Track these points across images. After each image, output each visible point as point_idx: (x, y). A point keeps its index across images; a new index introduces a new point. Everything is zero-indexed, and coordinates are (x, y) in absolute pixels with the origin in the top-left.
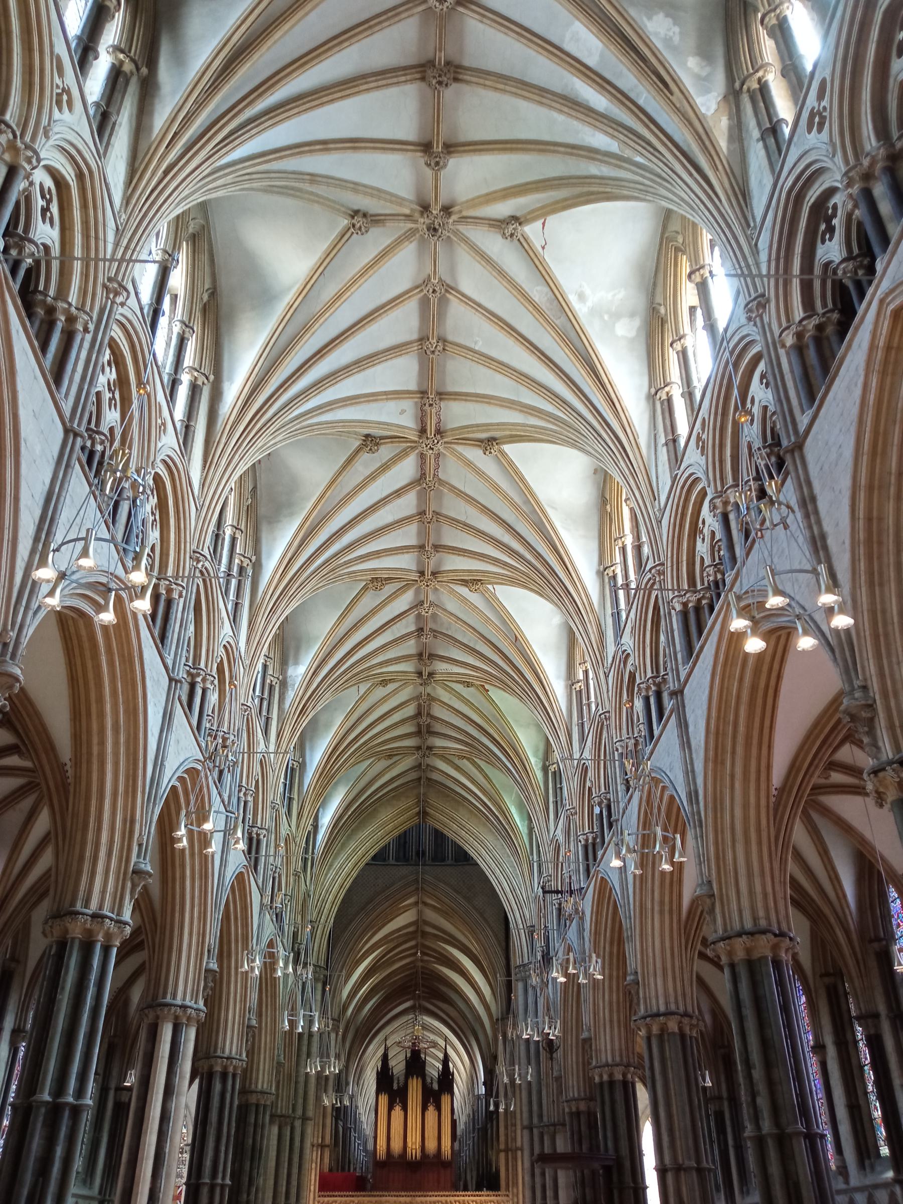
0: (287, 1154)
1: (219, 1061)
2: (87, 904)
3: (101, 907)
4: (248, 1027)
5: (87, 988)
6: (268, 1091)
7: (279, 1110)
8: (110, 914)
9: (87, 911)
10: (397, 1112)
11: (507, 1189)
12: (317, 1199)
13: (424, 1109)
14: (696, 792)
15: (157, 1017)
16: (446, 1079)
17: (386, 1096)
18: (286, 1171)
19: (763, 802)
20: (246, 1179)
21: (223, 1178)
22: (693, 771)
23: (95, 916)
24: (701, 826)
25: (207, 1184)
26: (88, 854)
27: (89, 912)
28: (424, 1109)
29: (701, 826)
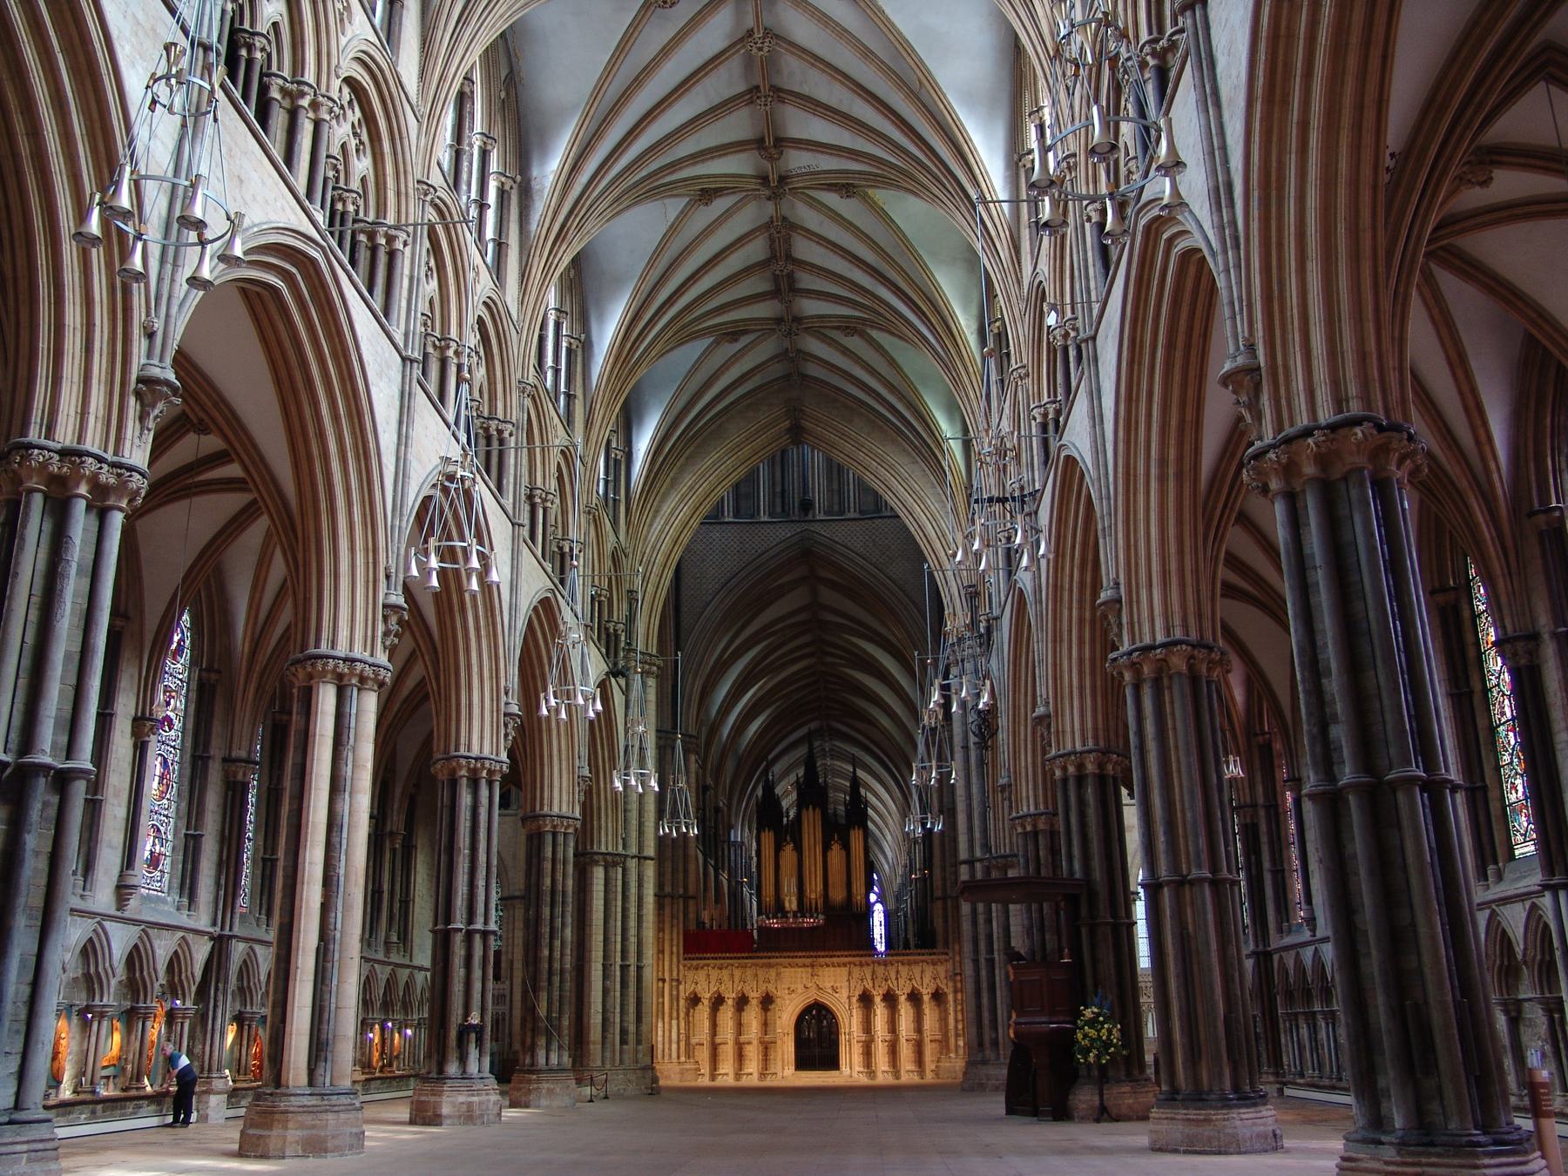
0: (619, 903)
1: (463, 762)
2: (50, 432)
3: (81, 438)
4: (505, 715)
5: (64, 576)
6: (570, 815)
7: (603, 847)
8: (101, 453)
9: (50, 444)
10: (788, 853)
11: (946, 944)
12: (682, 962)
13: (826, 848)
14: (1229, 186)
15: (310, 677)
16: (858, 813)
17: (772, 834)
18: (619, 924)
19: (1366, 171)
20: (546, 930)
21: (486, 922)
22: (1224, 147)
23: (65, 453)
24: (1237, 247)
25: (461, 930)
26: (43, 345)
27: (59, 446)
28: (826, 848)
29: (1237, 247)
